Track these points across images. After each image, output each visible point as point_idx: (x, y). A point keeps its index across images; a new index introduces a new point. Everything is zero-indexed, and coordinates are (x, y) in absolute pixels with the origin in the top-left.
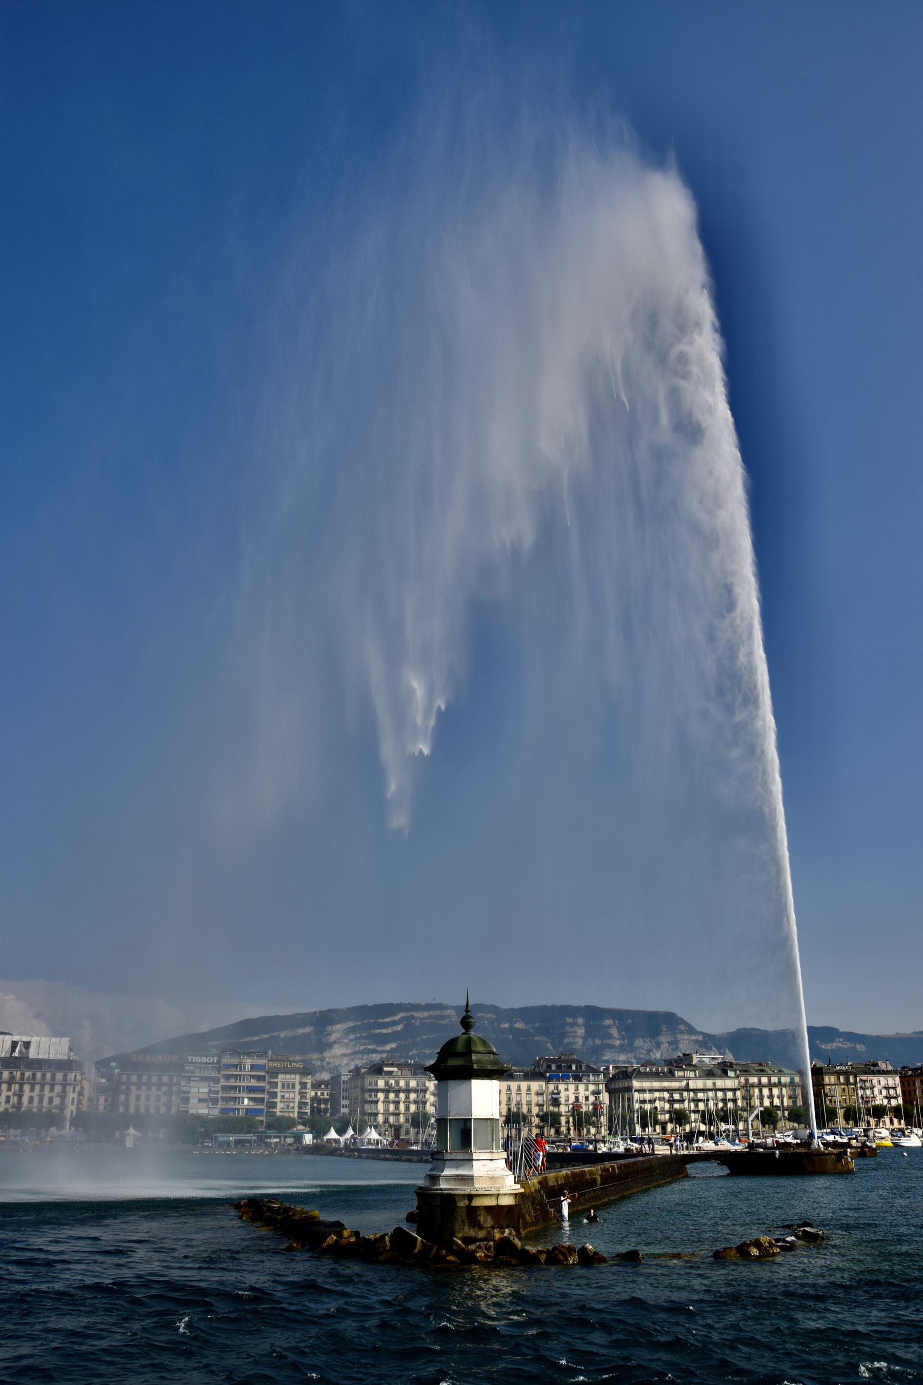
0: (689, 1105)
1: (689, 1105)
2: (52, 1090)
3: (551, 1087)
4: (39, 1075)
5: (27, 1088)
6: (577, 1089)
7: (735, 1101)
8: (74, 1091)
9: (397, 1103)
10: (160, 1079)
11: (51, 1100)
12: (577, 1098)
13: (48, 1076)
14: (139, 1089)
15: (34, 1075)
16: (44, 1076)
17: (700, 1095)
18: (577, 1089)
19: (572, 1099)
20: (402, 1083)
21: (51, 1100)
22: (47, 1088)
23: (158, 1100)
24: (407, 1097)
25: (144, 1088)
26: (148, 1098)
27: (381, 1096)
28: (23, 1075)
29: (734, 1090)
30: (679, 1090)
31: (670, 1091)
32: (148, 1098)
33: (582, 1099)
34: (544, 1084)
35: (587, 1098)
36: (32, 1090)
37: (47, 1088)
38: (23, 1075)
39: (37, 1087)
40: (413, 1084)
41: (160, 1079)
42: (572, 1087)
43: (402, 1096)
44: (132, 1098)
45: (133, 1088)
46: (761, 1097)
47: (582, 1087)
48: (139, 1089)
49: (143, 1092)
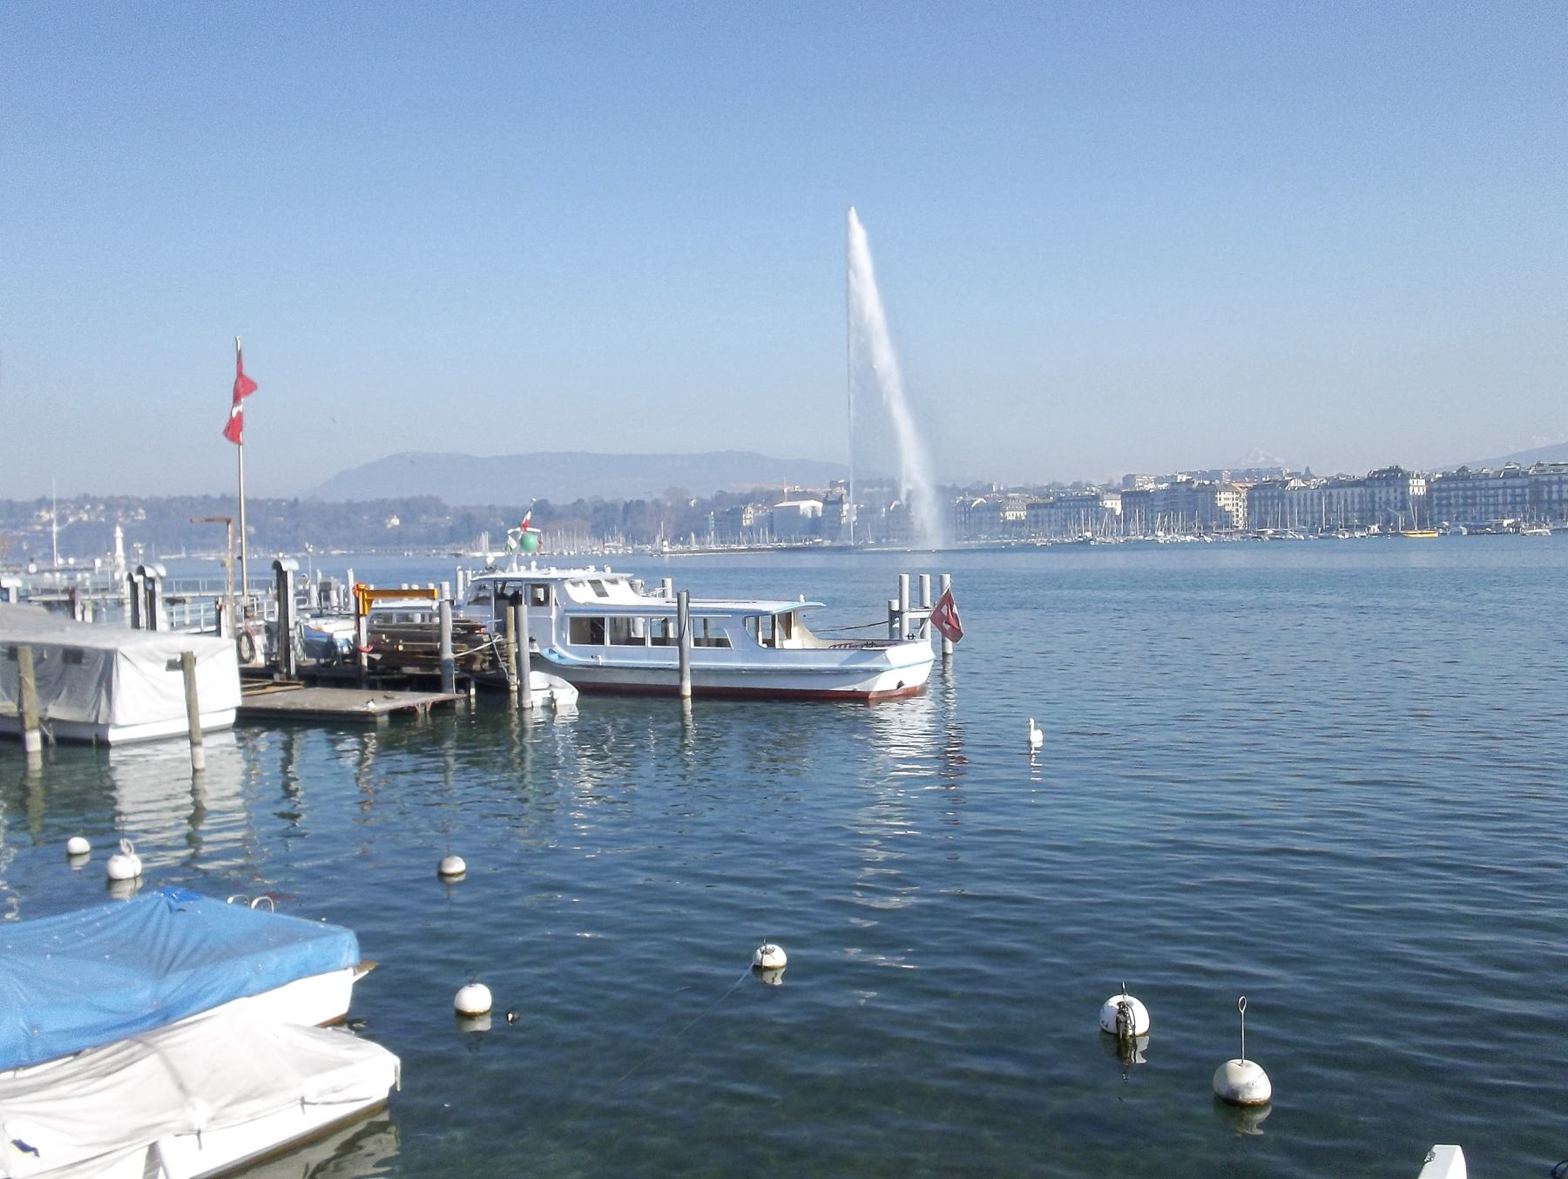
0: (1481, 500)
1: (1481, 500)
3: (1369, 491)
6: (1388, 492)
7: (1523, 495)
9: (1266, 506)
12: (1388, 499)
17: (1492, 492)
18: (1388, 492)
19: (1383, 499)
20: (1269, 494)
22: (1090, 510)
24: (1272, 503)
27: (1257, 502)
29: (1523, 487)
30: (1474, 488)
31: (1465, 489)
33: (1392, 498)
34: (1363, 489)
35: (1396, 498)
40: (1276, 494)
42: (1384, 492)
43: (1270, 502)
46: (1550, 492)
47: (1392, 490)
48: (1130, 506)
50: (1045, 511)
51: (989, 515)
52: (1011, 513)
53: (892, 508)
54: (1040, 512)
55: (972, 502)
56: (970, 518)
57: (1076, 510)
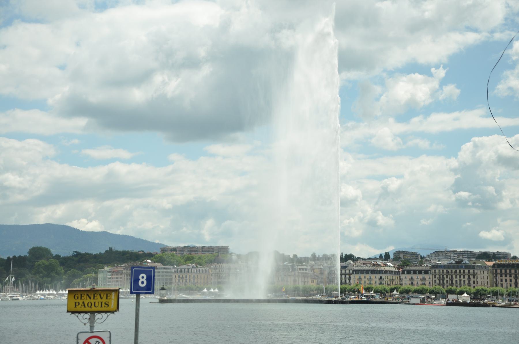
2: (464, 277)
4: (458, 271)
5: (454, 276)
8: (474, 278)
11: (464, 281)
13: (462, 271)
14: (501, 276)
15: (456, 271)
16: (460, 271)
21: (464, 281)
22: (462, 277)
23: (511, 281)
25: (504, 276)
26: (506, 280)
28: (452, 271)
32: (506, 280)
36: (456, 277)
37: (462, 277)
38: (452, 271)
39: (458, 276)
44: (499, 280)
45: (499, 276)
48: (501, 276)
49: (504, 278)
54: (415, 276)
56: (350, 279)
57: (449, 276)
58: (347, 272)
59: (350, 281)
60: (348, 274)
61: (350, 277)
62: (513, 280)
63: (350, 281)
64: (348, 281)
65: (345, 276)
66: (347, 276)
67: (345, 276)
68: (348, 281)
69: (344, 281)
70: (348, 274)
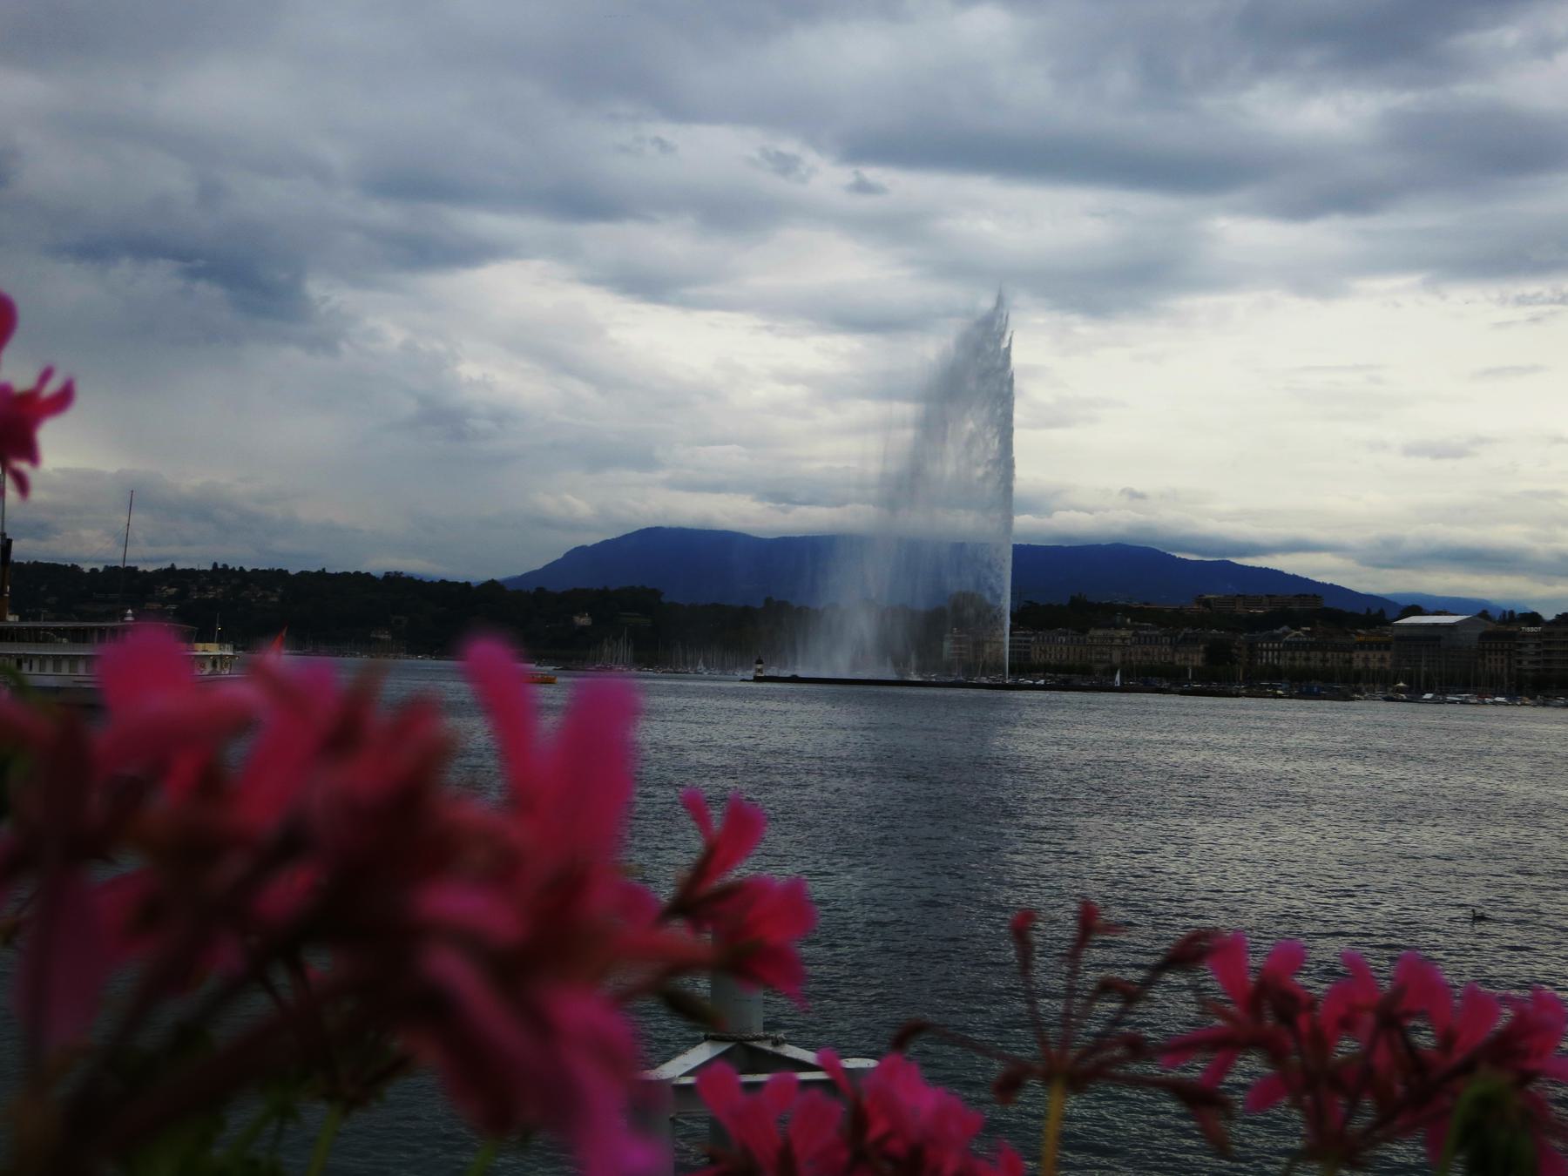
10: (1503, 646)
41: (1503, 646)
45: (1487, 653)
49: (1493, 657)
50: (1379, 655)
51: (1304, 654)
52: (1335, 654)
53: (1180, 637)
54: (1371, 655)
55: (1286, 634)
56: (1278, 659)
58: (1276, 645)
59: (1278, 663)
60: (1276, 650)
61: (1279, 655)
62: (1506, 661)
63: (1278, 663)
64: (1276, 661)
65: (1273, 654)
66: (1276, 653)
67: (1273, 654)
68: (1276, 661)
69: (1270, 660)
70: (1276, 650)
